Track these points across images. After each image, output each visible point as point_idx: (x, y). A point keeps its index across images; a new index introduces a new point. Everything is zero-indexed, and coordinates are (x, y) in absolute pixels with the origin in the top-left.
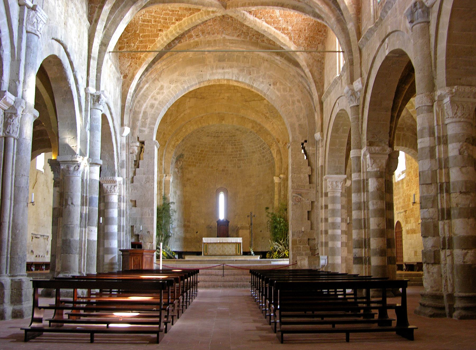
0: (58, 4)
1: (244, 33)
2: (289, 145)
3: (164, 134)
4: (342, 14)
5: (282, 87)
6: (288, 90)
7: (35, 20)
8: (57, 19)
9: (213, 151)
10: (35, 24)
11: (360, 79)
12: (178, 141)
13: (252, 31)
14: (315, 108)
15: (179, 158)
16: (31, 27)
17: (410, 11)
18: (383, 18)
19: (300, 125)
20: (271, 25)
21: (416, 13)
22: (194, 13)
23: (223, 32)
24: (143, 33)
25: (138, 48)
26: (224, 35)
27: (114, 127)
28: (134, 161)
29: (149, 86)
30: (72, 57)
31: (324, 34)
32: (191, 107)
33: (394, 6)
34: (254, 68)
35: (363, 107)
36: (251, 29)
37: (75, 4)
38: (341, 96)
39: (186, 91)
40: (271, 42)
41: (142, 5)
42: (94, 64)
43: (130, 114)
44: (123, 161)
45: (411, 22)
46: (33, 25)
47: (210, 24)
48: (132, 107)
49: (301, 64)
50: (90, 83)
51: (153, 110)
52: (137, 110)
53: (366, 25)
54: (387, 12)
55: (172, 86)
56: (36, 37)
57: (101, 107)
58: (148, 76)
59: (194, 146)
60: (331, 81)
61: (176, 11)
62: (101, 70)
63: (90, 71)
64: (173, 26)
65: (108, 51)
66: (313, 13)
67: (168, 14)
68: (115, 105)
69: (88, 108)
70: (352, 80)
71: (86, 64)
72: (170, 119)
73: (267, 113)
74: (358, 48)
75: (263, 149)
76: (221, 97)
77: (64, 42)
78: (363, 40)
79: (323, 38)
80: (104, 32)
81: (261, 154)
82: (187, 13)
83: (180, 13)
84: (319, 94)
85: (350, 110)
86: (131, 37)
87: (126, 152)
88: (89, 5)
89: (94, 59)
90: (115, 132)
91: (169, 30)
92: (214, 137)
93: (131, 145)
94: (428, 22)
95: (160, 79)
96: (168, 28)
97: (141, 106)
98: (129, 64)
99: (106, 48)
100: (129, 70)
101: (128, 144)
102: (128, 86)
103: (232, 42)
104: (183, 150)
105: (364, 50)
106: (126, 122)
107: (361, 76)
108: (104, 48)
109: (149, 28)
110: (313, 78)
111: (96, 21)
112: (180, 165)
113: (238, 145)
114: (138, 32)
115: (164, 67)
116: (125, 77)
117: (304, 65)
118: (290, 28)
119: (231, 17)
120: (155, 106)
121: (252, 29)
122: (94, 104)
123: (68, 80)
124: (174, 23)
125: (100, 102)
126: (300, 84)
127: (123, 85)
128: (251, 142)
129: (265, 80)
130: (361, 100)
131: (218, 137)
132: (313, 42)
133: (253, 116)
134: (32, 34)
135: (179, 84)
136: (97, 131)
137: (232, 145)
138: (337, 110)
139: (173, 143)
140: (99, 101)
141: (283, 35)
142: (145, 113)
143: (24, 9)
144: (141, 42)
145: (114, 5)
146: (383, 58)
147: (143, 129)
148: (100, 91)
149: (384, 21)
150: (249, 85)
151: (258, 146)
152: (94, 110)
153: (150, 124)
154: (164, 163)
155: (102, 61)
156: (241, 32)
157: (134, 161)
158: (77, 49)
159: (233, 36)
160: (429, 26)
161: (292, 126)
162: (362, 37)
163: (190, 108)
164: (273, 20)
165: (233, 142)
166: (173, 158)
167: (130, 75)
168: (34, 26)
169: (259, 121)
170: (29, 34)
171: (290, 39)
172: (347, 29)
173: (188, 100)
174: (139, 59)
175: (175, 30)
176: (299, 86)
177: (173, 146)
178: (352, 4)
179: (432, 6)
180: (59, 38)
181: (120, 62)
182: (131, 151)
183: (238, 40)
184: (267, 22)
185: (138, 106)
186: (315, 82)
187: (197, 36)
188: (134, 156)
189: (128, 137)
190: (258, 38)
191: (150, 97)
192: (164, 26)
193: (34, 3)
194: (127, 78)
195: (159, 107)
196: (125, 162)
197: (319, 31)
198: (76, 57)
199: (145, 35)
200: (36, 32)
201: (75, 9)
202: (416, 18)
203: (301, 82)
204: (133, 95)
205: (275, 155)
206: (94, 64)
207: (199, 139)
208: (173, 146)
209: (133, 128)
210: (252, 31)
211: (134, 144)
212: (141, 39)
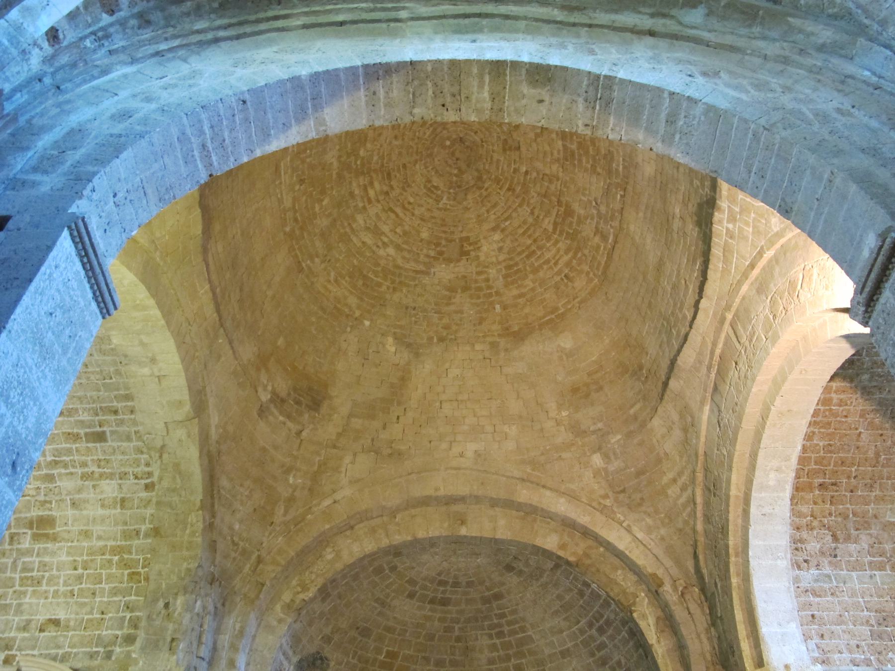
3: (259, 560)
9: (427, 660)
12: (305, 588)
32: (358, 481)
59: (365, 632)
72: (285, 515)
73: (606, 496)
75: (601, 631)
76: (456, 450)
81: (592, 655)
97: (64, 109)
104: (327, 639)
113: (513, 633)
128: (556, 613)
131: (444, 602)
133: (561, 506)
137: (490, 637)
139: (287, 597)
151: (583, 622)
163: (353, 482)
165: (495, 621)
173: (348, 459)
177: (288, 607)
205: (651, 634)
207: (383, 604)
208: (288, 607)
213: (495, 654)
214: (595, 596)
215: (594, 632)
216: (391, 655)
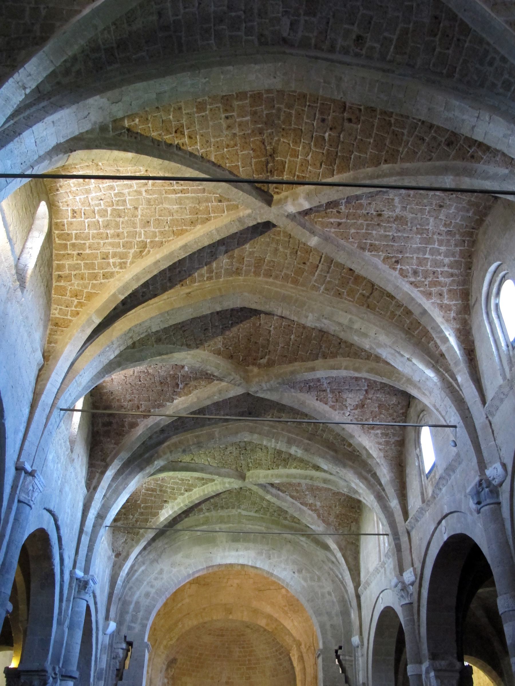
0: (57, 467)
1: (264, 508)
2: (319, 652)
4: (384, 490)
5: (308, 575)
6: (316, 580)
7: (31, 488)
8: (53, 486)
10: (30, 492)
11: (412, 569)
12: (171, 639)
13: (273, 506)
14: (350, 602)
15: (171, 663)
16: (24, 496)
17: (475, 490)
18: (436, 496)
19: (331, 625)
20: (296, 500)
21: (483, 492)
22: (207, 483)
23: (239, 507)
24: (146, 503)
25: (137, 521)
26: (239, 510)
27: (97, 622)
28: (117, 670)
29: (146, 569)
30: (61, 532)
31: (358, 511)
33: (449, 483)
34: (274, 551)
35: (419, 606)
36: (272, 505)
37: (75, 468)
38: (386, 589)
39: (190, 577)
40: (295, 520)
41: (149, 472)
42: (85, 540)
43: (118, 604)
44: (102, 670)
45: (479, 503)
46: (28, 494)
47: (224, 496)
48: (122, 596)
49: (332, 548)
50: (78, 565)
51: (148, 601)
52: (127, 598)
53: (414, 503)
54: (440, 489)
55: (175, 570)
56: (28, 508)
57: (87, 597)
58: (145, 557)
59: (191, 648)
60: (371, 570)
61: (186, 480)
62: (93, 548)
63: (80, 549)
64: (181, 497)
65: (104, 525)
66: (347, 487)
67: (177, 483)
68: (102, 591)
69: (71, 596)
70: (401, 570)
71: (76, 539)
73: (285, 606)
74: (405, 530)
77: (56, 513)
78: (413, 521)
79: (357, 516)
80: (103, 501)
81: (277, 661)
82: (199, 483)
83: (190, 482)
84: (355, 585)
85: (401, 608)
86: (130, 507)
87: (108, 657)
88: (88, 470)
89: (87, 534)
90: (97, 628)
91: (176, 501)
92: (218, 635)
93: (115, 646)
94: (499, 503)
95: (160, 561)
96: (175, 499)
97: (133, 595)
98: (124, 539)
99: (103, 522)
100: (124, 548)
101: (111, 645)
102: (121, 567)
103: (249, 518)
104: (178, 652)
105: (413, 534)
106: (112, 614)
107: (413, 566)
108: (100, 521)
109: (153, 498)
110: (347, 565)
111: (95, 489)
112: (172, 674)
114: (139, 502)
115: (166, 546)
116: (118, 555)
117: (335, 549)
118: (318, 504)
119: (250, 489)
120: (151, 595)
121: (274, 504)
122: (79, 592)
123: (52, 560)
124: (182, 494)
125: (86, 591)
126: (331, 572)
127: (113, 567)
129: (288, 567)
130: (416, 596)
132: (346, 521)
133: (268, 609)
134: (25, 505)
135: (182, 568)
136: (78, 630)
137: (240, 648)
138: (380, 607)
139: (165, 642)
140: (85, 588)
141: (310, 512)
142: (137, 603)
143: (20, 474)
144: (142, 514)
145: (118, 470)
146: (441, 544)
147: (133, 625)
148: (89, 576)
149: (437, 499)
150: (268, 572)
151: (274, 649)
152: (78, 600)
153: (142, 619)
154: (152, 670)
155: (96, 537)
156: (260, 507)
157: (117, 670)
158: (68, 521)
159: (251, 511)
160: (500, 509)
161: (322, 627)
162: (410, 517)
163: (190, 596)
164: (298, 494)
166: (164, 664)
167: (124, 554)
168: (28, 494)
169: (276, 615)
170: (21, 504)
171: (319, 516)
172: (390, 507)
174: (137, 535)
175: (183, 502)
176: (329, 574)
178: (394, 478)
179: (501, 484)
180: (52, 508)
181: (113, 536)
182: (114, 655)
183: (256, 517)
184: (292, 497)
185: (130, 593)
186: (350, 570)
187: (208, 510)
188: (116, 663)
189: (112, 635)
190: (279, 515)
191: (145, 583)
192: (170, 497)
193: (33, 468)
194: (120, 557)
195: (156, 596)
196: (104, 672)
197: (352, 508)
198: (66, 531)
199: (147, 506)
200: (29, 502)
201: (73, 474)
202: (484, 498)
203: (332, 570)
204: (125, 580)
205: (295, 663)
206: (85, 540)
208: (165, 647)
209: (120, 623)
210: (273, 506)
211: (120, 646)
212: (142, 510)
213: (241, 654)
214: (279, 643)
215: (278, 653)
216: (201, 654)
